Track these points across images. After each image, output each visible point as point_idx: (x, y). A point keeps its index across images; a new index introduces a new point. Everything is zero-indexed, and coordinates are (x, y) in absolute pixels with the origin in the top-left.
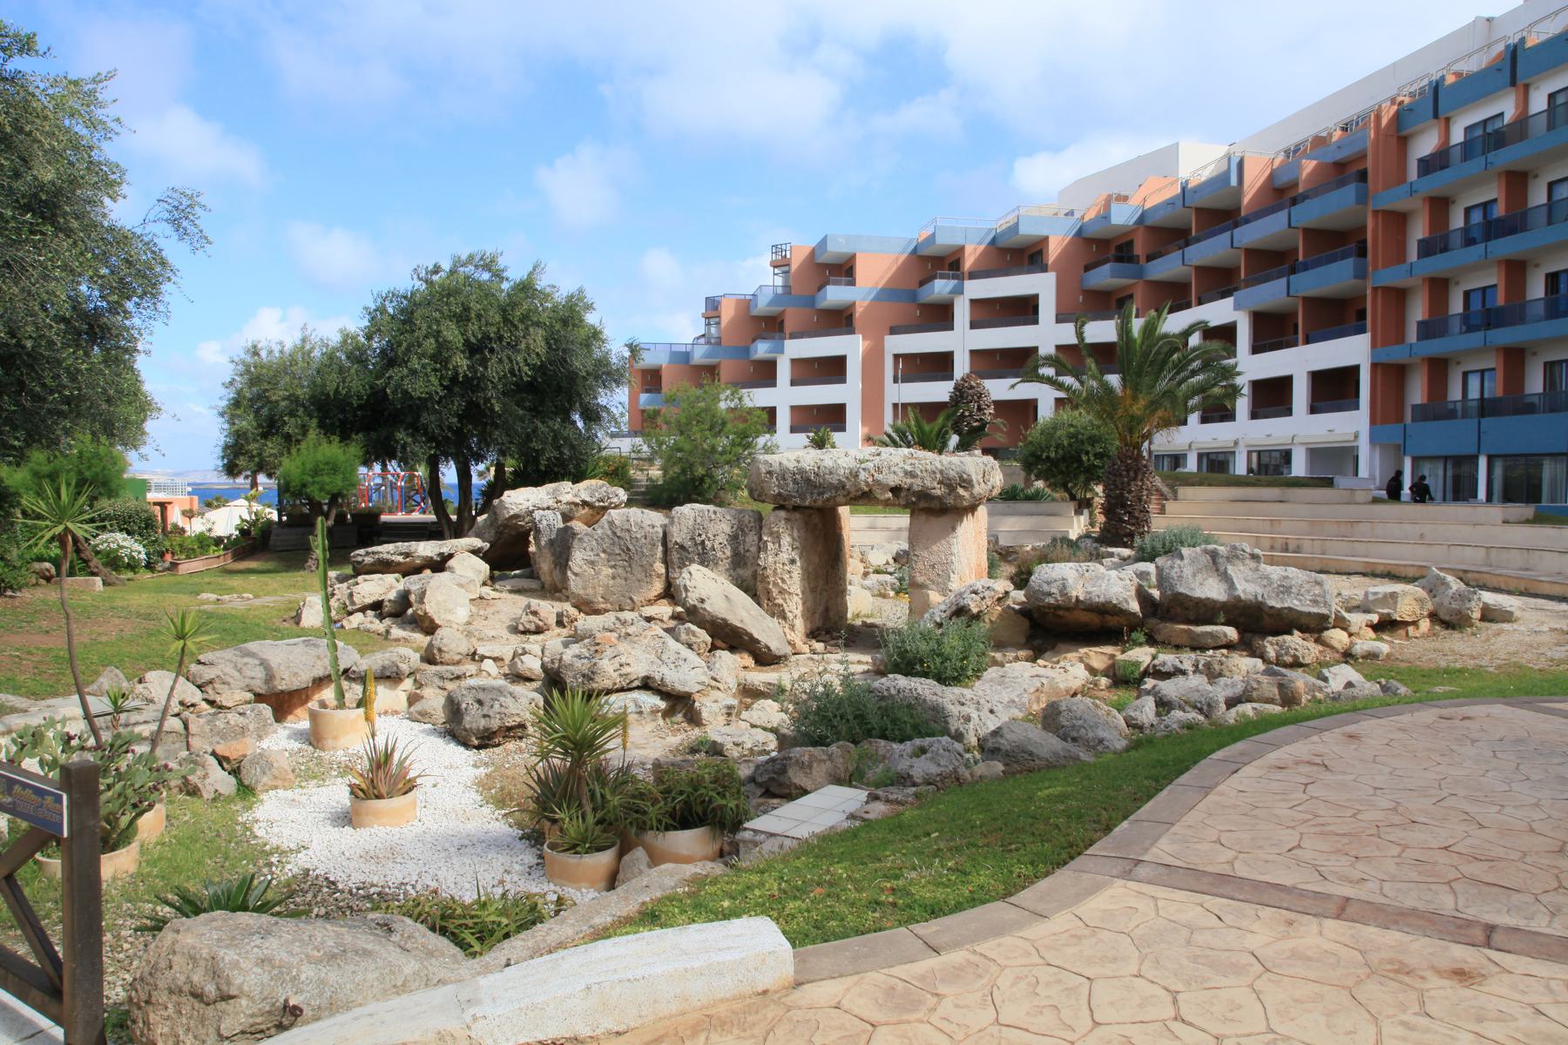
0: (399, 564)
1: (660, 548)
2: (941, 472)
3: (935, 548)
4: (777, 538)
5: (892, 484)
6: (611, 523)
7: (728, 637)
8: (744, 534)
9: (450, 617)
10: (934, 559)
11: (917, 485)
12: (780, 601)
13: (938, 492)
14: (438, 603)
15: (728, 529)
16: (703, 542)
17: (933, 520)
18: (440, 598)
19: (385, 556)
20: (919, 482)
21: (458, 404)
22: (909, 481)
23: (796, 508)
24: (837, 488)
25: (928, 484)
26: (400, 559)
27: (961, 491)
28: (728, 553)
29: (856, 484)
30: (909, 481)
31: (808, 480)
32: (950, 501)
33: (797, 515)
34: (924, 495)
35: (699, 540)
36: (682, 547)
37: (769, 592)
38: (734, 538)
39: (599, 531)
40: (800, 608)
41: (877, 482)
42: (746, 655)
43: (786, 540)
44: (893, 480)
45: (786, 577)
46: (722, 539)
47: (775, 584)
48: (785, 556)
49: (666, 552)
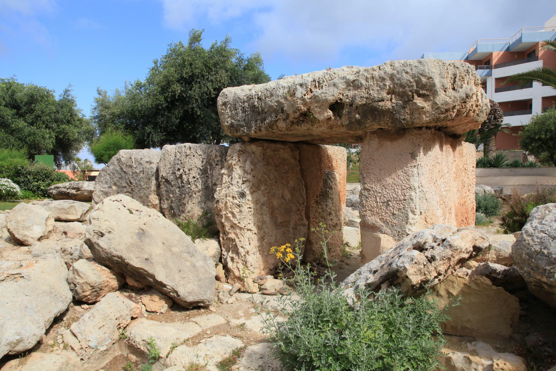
0: (74, 195)
1: (154, 182)
2: (392, 77)
3: (389, 180)
4: (230, 168)
5: (331, 99)
6: (119, 160)
7: (133, 280)
8: (212, 169)
9: (27, 233)
10: (388, 194)
11: (360, 97)
12: (232, 236)
13: (388, 105)
14: (18, 222)
15: (199, 164)
16: (181, 175)
17: (388, 144)
18: (19, 218)
19: (63, 190)
20: (363, 93)
21: (178, 112)
22: (351, 93)
23: (253, 140)
24: (276, 112)
25: (374, 94)
26: (74, 192)
27: (419, 102)
28: (200, 187)
29: (293, 104)
30: (351, 93)
31: (253, 107)
32: (405, 116)
33: (253, 147)
34: (370, 110)
35: (178, 173)
36: (167, 181)
37: (223, 226)
38: (204, 172)
39: (111, 167)
40: (255, 242)
41: (315, 98)
42: (156, 298)
43: (238, 171)
44: (331, 94)
45: (236, 210)
46: (195, 173)
47: (227, 218)
48: (235, 189)
49: (158, 186)
